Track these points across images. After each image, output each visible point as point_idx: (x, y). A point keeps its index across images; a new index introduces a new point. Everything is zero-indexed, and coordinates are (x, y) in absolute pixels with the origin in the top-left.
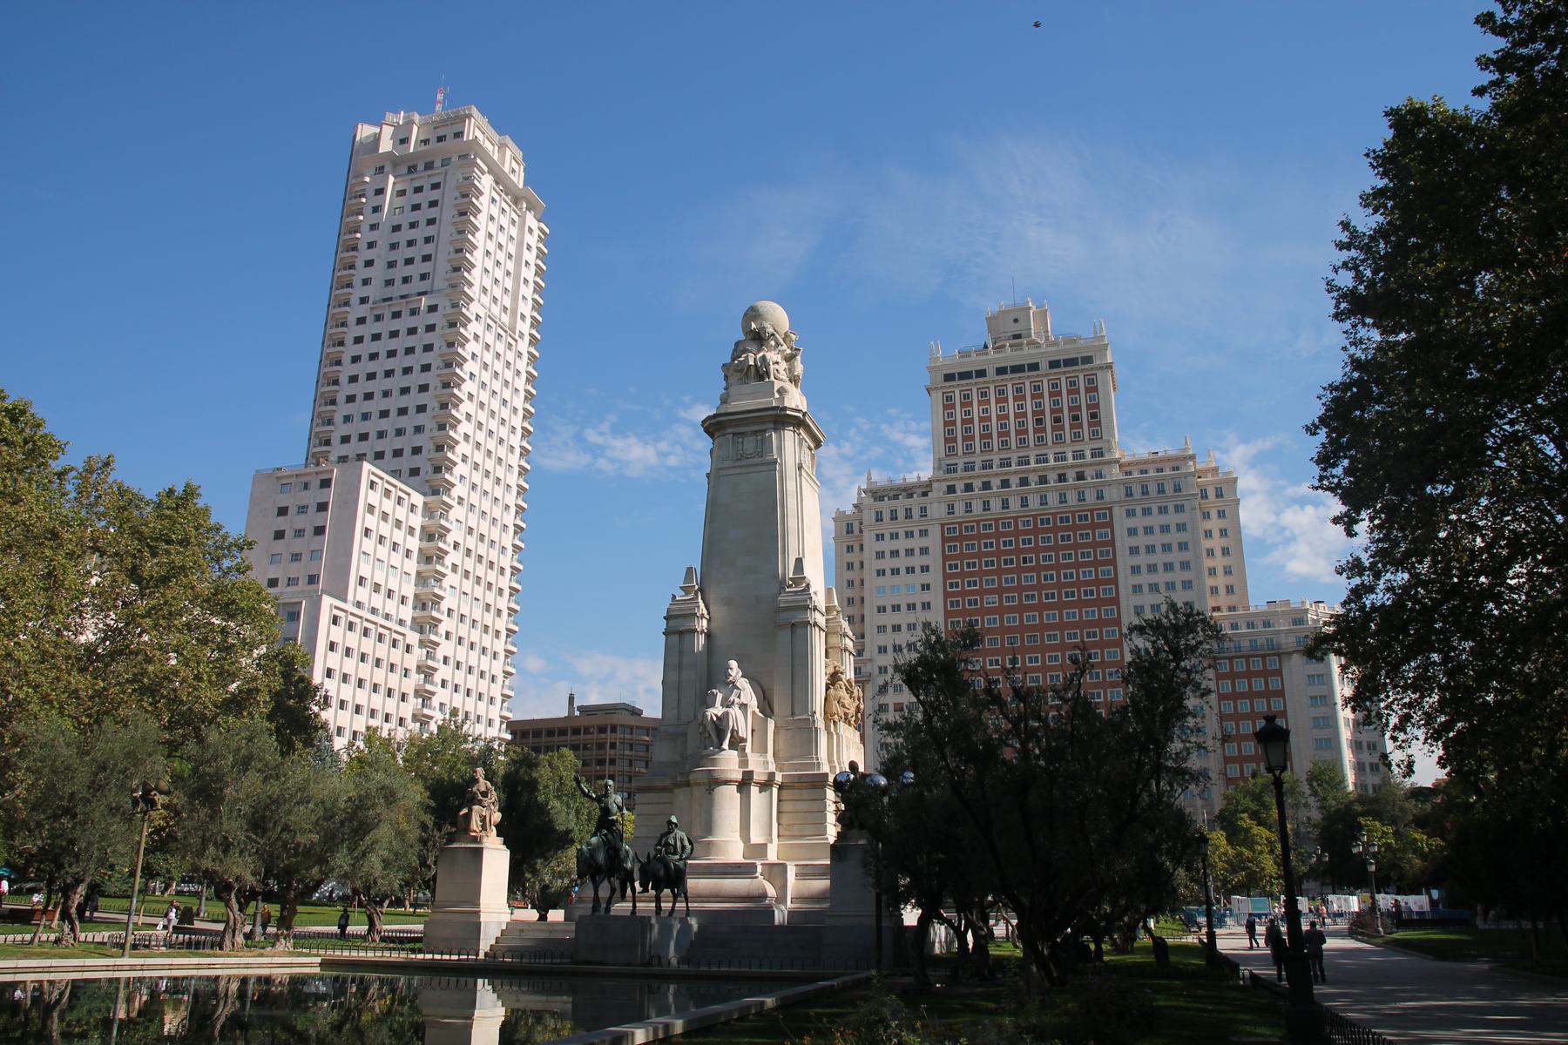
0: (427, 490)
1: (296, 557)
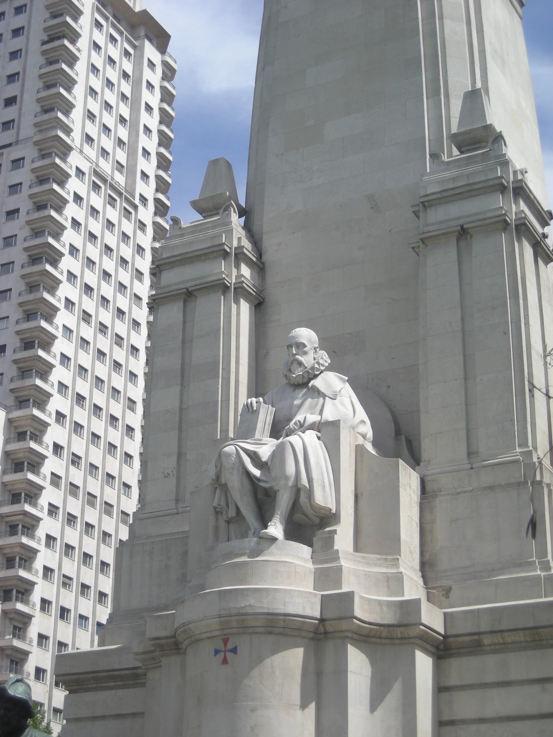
0: (11, 401)
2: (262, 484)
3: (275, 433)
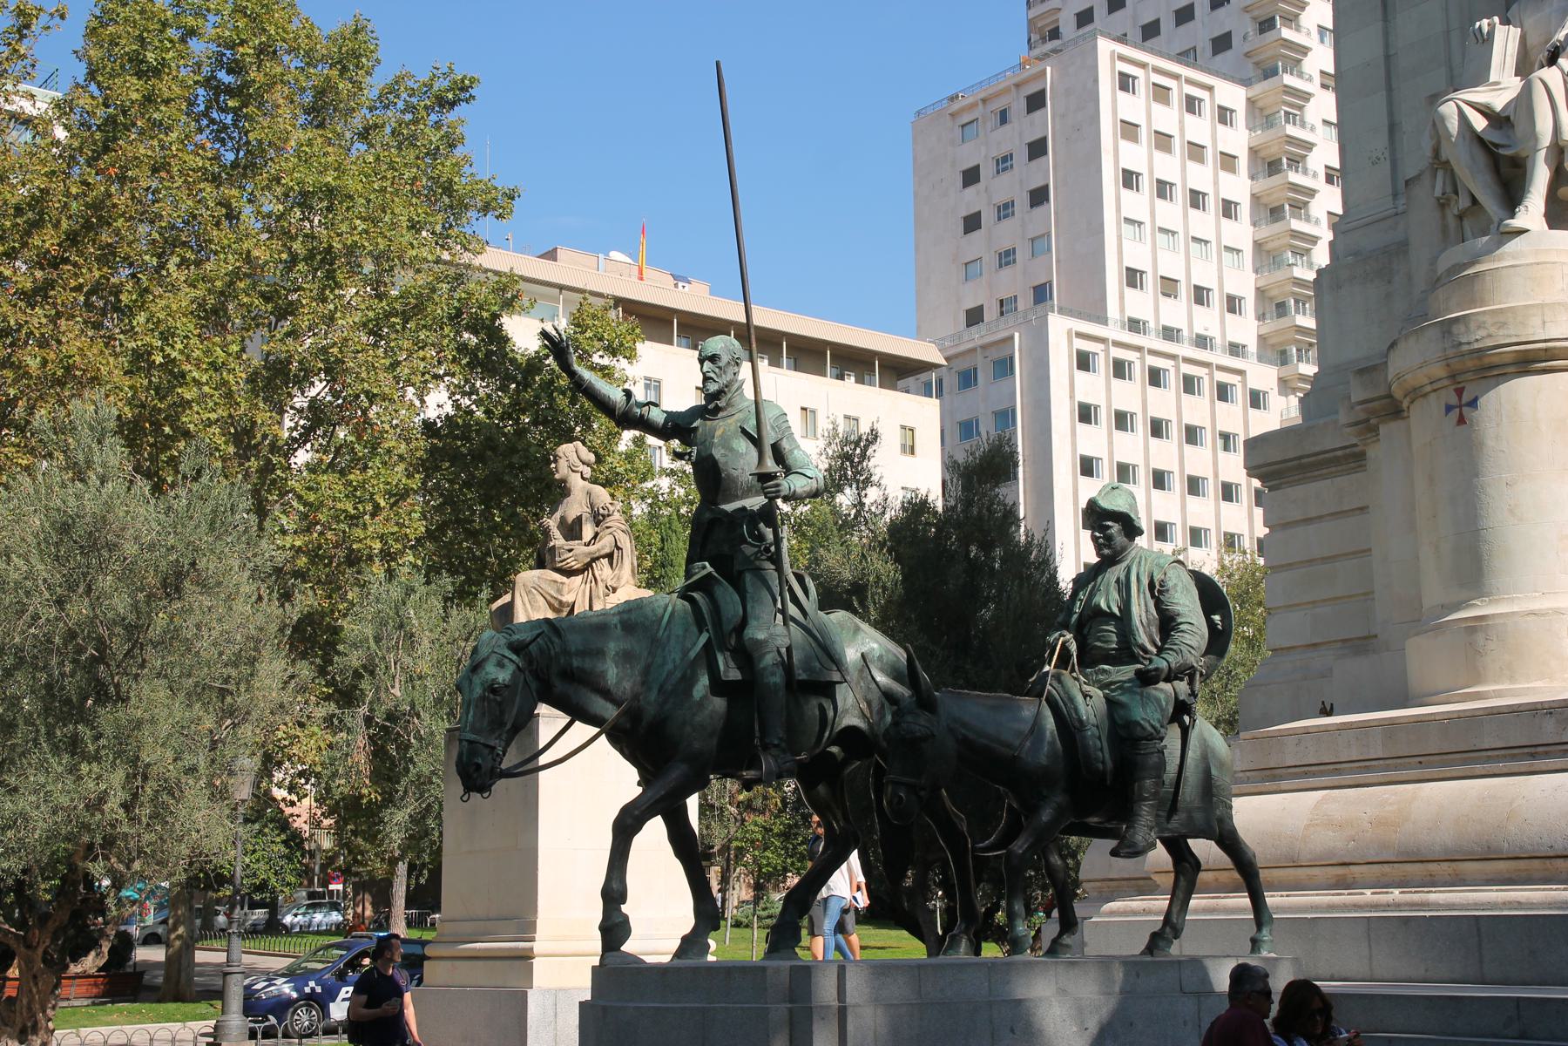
0: (1250, 71)
1: (1006, 258)
2: (1501, 151)
3: (1524, 67)
